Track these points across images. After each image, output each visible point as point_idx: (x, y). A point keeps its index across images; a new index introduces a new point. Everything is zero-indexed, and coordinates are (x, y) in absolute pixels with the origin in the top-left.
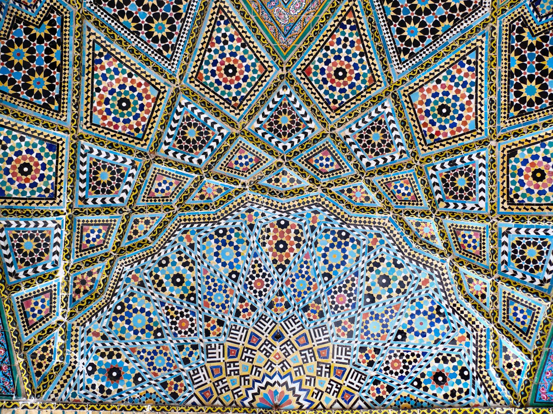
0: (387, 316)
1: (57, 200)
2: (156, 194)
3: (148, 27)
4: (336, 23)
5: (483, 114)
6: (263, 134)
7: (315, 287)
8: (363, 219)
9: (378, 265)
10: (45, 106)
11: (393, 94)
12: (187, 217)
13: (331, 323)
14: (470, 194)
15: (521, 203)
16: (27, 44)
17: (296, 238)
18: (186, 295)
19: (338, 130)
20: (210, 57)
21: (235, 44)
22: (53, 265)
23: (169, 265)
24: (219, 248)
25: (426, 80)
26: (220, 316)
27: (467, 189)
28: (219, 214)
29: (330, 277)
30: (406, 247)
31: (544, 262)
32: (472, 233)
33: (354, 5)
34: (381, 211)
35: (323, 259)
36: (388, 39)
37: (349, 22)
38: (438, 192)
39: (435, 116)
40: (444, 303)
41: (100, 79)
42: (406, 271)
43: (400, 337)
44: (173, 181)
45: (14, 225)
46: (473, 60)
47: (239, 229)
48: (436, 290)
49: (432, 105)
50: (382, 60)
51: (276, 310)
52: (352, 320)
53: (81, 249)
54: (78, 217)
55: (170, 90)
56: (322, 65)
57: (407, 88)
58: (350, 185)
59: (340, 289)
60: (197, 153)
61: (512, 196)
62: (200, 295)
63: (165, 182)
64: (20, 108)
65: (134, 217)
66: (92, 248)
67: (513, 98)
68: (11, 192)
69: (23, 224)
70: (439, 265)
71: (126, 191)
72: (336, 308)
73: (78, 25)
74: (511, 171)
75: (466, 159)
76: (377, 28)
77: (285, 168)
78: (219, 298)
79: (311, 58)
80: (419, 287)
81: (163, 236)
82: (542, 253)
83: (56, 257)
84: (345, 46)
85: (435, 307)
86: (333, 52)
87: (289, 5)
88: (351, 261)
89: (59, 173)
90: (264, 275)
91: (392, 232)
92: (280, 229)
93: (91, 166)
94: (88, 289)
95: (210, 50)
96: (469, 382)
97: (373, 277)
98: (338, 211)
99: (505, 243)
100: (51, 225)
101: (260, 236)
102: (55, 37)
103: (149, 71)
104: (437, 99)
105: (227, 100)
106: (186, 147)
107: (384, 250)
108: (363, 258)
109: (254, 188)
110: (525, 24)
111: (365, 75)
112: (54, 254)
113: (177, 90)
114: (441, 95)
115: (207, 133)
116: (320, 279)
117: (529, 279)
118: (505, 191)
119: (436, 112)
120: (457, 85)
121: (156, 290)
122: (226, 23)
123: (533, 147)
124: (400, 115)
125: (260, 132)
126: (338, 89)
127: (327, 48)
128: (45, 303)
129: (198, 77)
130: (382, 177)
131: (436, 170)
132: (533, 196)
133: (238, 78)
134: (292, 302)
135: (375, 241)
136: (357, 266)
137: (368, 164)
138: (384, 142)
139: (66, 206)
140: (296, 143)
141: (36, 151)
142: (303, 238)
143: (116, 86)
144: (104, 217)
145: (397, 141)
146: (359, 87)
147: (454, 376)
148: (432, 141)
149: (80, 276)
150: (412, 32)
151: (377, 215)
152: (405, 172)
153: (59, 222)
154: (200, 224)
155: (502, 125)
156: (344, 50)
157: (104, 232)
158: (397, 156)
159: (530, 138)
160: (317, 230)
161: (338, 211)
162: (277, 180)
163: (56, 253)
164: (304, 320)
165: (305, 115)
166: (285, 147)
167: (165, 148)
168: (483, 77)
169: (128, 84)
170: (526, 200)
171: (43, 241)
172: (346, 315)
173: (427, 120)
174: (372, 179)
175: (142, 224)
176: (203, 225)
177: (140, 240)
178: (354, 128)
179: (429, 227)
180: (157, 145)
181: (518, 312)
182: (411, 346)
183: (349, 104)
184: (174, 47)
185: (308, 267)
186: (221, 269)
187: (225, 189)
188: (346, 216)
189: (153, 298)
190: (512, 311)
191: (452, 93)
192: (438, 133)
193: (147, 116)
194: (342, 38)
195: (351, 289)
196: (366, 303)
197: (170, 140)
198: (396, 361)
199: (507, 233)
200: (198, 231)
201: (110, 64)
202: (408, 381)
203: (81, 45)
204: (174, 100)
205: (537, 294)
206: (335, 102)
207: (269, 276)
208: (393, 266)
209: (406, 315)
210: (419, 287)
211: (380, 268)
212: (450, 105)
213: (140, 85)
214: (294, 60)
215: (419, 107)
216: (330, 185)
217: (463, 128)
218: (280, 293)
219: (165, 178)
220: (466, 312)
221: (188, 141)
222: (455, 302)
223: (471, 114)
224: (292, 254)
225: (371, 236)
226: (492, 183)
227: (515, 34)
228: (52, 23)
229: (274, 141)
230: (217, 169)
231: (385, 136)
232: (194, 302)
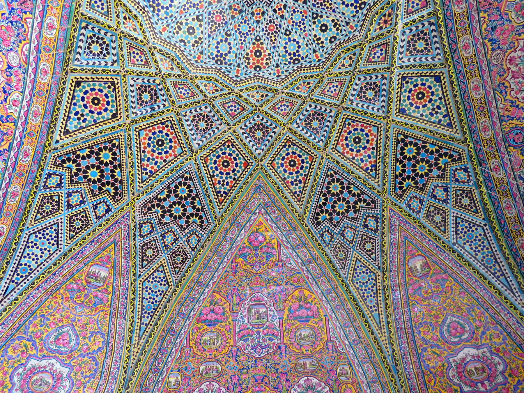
1: (401, 76)
2: (337, 84)
3: (343, 188)
5: (135, 141)
6: (271, 124)
7: (235, 26)
8: (207, 72)
9: (196, 42)
10: (406, 137)
12: (318, 70)
14: (140, 89)
15: (106, 83)
16: (417, 175)
17: (249, 59)
18: (319, 18)
19: (226, 128)
20: (305, 171)
21: (290, 180)
22: (405, 32)
23: (329, 38)
24: (298, 51)
25: (173, 161)
26: (297, 5)
27: (142, 92)
28: (298, 73)
29: (226, 34)
30: (178, 54)
31: (87, 42)
32: (136, 62)
35: (231, 46)
37: (222, 196)
38: (161, 90)
39: (166, 139)
40: (150, 14)
41: (372, 156)
42: (178, 37)
44: (327, 93)
45: (429, 58)
46: (144, 175)
47: (285, 64)
48: (157, 24)
49: (168, 146)
51: (260, 10)
53: (386, 45)
54: (387, 66)
55: (329, 150)
56: (237, 169)
58: (216, 94)
59: (219, 26)
60: (312, 111)
61: (113, 87)
62: (310, 18)
63: (332, 92)
64: (422, 134)
65: (352, 69)
66: (379, 46)
67: (118, 152)
68: (430, 80)
69: (423, 59)
70: (156, 41)
71: (357, 85)
72: (221, 12)
73: (385, 187)
74: (115, 104)
77: (258, 104)
78: (297, 17)
80: (168, 26)
81: (333, 57)
83: (403, 38)
86: (231, 177)
88: (213, 45)
89: (399, 94)
90: (268, 35)
91: (189, 64)
92: (259, 65)
93: (379, 100)
94: (383, 18)
95: (305, 175)
97: (198, 34)
98: (223, 78)
99: (115, 55)
100: (405, 60)
101: (271, 60)
102: (399, 179)
103: (342, 161)
104: (165, 150)
105: (294, 145)
106: (319, 115)
107: (192, 52)
108: (206, 46)
109: (276, 90)
110: (114, 197)
111: (211, 163)
112: (404, 40)
113: (325, 150)
115: (306, 124)
116: (233, 32)
117: (96, 30)
118: (117, 91)
120: (153, 159)
121: (338, 20)
122: (296, 192)
123: (101, 120)
124: (188, 139)
125: (274, 126)
126: (227, 155)
127: (234, 179)
128: (412, 5)
129: (312, 158)
130: (197, 100)
131: (163, 104)
132: (99, 88)
133: (288, 159)
134: (250, 16)
135: (199, 58)
136: (209, 41)
137: (206, 108)
138: (197, 122)
139: (395, 73)
140: (251, 120)
141: (413, 108)
143: (362, 151)
144: (371, 67)
145: (189, 123)
146: (214, 156)
148: (167, 123)
149: (388, 26)
150: (183, 191)
151: (199, 75)
152: (183, 103)
153: (400, 62)
154: (310, 66)
155: (123, 134)
156: (224, 178)
157: (371, 57)
158: (188, 113)
159: (104, 126)
160: (236, 65)
161: (223, 78)
162: (262, 96)
163: (402, 41)
164: (242, 4)
165: (246, 138)
166: (258, 117)
167: (332, 114)
168: (137, 164)
169: (354, 153)
170: (103, 85)
171: (411, 49)
172: (214, 7)
173: (171, 137)
174: (203, 98)
175: (347, 64)
176: (308, 66)
177: (348, 53)
178: (216, 130)
179: (165, 66)
180: (337, 115)
181: (101, 6)
184: (327, 176)
185: (241, 40)
186: (296, 37)
187: (294, 89)
188: (218, 74)
189: (340, 15)
190: (105, 7)
191: (156, 154)
192: (163, 128)
193: (343, 133)
194: (225, 186)
195: (212, 25)
196: (202, 15)
197: (329, 119)
199: (114, 62)
200: (311, 62)
201: (366, 165)
203: (384, 175)
204: (327, 144)
205: (90, 18)
206: (228, 146)
207: (265, 34)
208: (186, 41)
209: (175, 6)
211: (194, 40)
212: (157, 146)
213: (348, 153)
214: (254, 171)
215: (176, 145)
216: (230, 94)
217: (147, 132)
218: (258, 22)
219: (332, 94)
220: (136, 7)
221: (317, 119)
222: (144, 15)
223: (143, 141)
224: (251, 49)
225: (202, 61)
227: (119, 191)
228: (401, 188)
229: (265, 121)
230: (300, 101)
231: (197, 126)
232: (313, 13)
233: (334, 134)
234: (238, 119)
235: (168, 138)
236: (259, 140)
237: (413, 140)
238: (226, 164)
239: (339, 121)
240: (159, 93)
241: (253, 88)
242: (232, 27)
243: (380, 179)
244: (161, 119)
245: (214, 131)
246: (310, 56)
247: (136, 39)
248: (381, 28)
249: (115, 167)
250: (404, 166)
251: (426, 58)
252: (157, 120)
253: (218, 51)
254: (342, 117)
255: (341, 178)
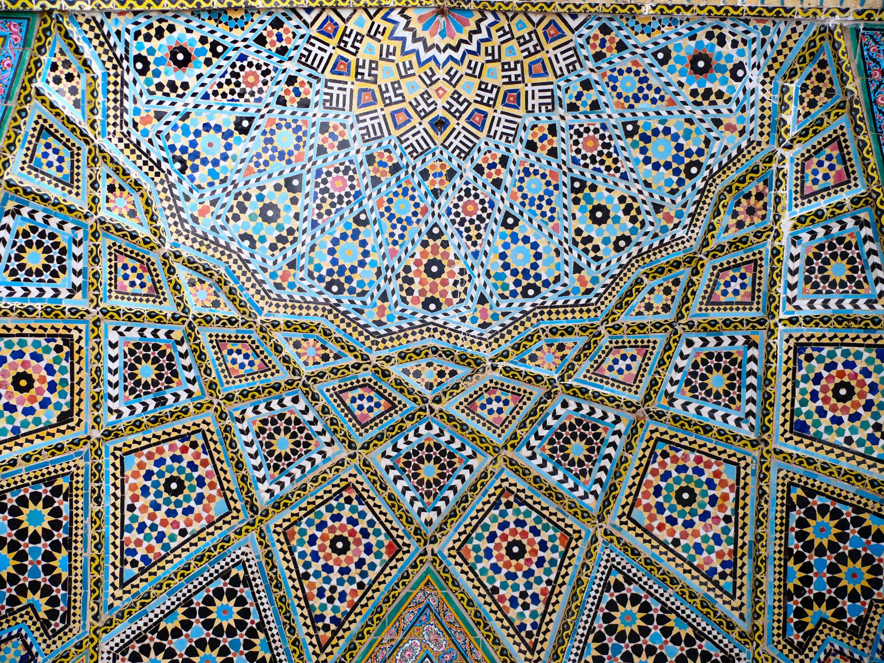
0: (266, 156)
1: (792, 342)
2: (634, 351)
3: (648, 619)
4: (346, 625)
5: (112, 480)
6: (463, 448)
7: (380, 203)
8: (304, 312)
9: (281, 239)
10: (812, 493)
11: (256, 513)
13: (355, 146)
14: (132, 352)
15: (51, 338)
17: (410, 281)
18: (587, 190)
20: (548, 572)
21: (508, 593)
22: (798, 238)
23: (613, 239)
24: (535, 266)
26: (533, 158)
27: (138, 360)
28: (534, 320)
29: (357, 220)
30: (234, 267)
31: (15, 243)
32: (130, 290)
33: (318, 656)
34: (275, 325)
35: (368, 248)
36: (265, 600)
37: (326, 628)
38: (184, 356)
39: (189, 477)
40: (173, 178)
42: (235, 229)
43: (245, 124)
44: (607, 373)
45: (861, 303)
46: (128, 567)
47: (502, 296)
48: (187, 199)
49: (194, 495)
50: (274, 567)
51: (443, 166)
52: (321, 150)
53: (755, 264)
54: (759, 315)
55: (612, 520)
56: (369, 559)
57: (234, 522)
58: (324, 367)
59: (340, 201)
60: (569, 417)
61: (66, 349)
62: (565, 190)
63: (620, 371)
64: (852, 490)
65: (670, 316)
66: (737, 266)
67: (65, 507)
68: (866, 355)
69: (847, 303)
70: (182, 239)
71: (683, 357)
72: (347, 170)
73: (759, 623)
74: (68, 389)
75: (139, 408)
76: (282, 619)
77: (429, 395)
78: (534, 186)
79: (387, 571)
80: (214, 203)
81: (624, 285)
82: (18, 258)
83: (795, 251)
84: (333, 589)
85: (188, 172)
86: (352, 580)
87: (423, 654)
88: (323, 245)
89: (789, 386)
90: (462, 223)
91: (258, 292)
92: (437, 296)
93: (739, 397)
94: (744, 202)
95: (549, 582)
96: (134, 52)
97: (287, 220)
98: (343, 326)
99: (77, 273)
100: (802, 303)
101: (468, 285)
102: (795, 603)
103: (646, 550)
104: (185, 505)
105: (522, 503)
106: (586, 427)
107: (270, 262)
108: (305, 249)
109: (478, 362)
110: (45, 624)
111: (301, 543)
112: (798, 256)
113: (601, 518)
114: (180, 510)
115: (554, 450)
116: (373, 216)
117: (39, 217)
118: (76, 357)
119: (187, 484)
120: (154, 527)
121: (634, 199)
122: (523, 626)
123: (32, 427)
124: (244, 479)
125: (468, 451)
126: (344, 521)
127: (361, 585)
128: (812, 177)
129: (568, 539)
130: (272, 380)
131: (187, 391)
132: (32, 350)
133: (504, 537)
134: (417, 178)
135: (284, 277)
136: (313, 237)
137: (295, 400)
138: (271, 436)
141: (826, 422)
142: (400, 281)
143: (699, 525)
144: (718, 315)
146: (310, 523)
147: (158, 62)
149: (757, 220)
150: (225, 611)
151: (281, 318)
152: (236, 388)
153: (789, 307)
155: (81, 463)
156: (334, 583)
158: (249, 414)
159: (38, 442)
160: (377, 294)
161: (343, 326)
162: (441, 374)
163: (794, 258)
164: (398, 151)
165: (396, 479)
166: (429, 427)
168: (112, 539)
169: (679, 528)
170: (44, 343)
171: (816, 277)
172: (330, 159)
173: (202, 471)
174: (289, 376)
175: (658, 305)
176: (560, 303)
177: (659, 280)
178: (318, 458)
179: (198, 299)
180: (634, 431)
181: (56, 164)
182: (228, 108)
183: (326, 496)
184: (607, 587)
185: (392, 235)
188: (331, 317)
189: (640, 186)
191: (161, 514)
192: (184, 450)
193: (649, 477)
194: (337, 603)
195: (323, 200)
196: (299, 177)
198: (251, 85)
200: (567, 293)
201: (708, 561)
202: (231, 53)
204: (606, 503)
206: (349, 500)
208: (256, 237)
209: (234, 158)
210: (214, 203)
211: (277, 233)
212: (165, 495)
213: (661, 527)
214: (414, 566)
215: (214, 492)
216: (357, 367)
217: (144, 459)
218: (436, 193)
219: (620, 378)
220: (140, 163)
221: (583, 437)
222: (157, 179)
223: (132, 480)
224: (418, 256)
225: (292, 286)
226: (98, 370)
227: (61, 608)
228: (800, 626)
229: (447, 437)
230: (538, 392)
231: (269, 445)
232: (573, 180)
233: (627, 479)
234: (375, 432)
235: (196, 475)
236: (429, 485)
237: (828, 502)
238: (340, 545)
239: (639, 446)
240: (179, 362)
241: (417, 352)
242: (371, 203)
243: (745, 599)
244: (179, 426)
245: (312, 461)
246: (566, 280)
247: (134, 237)
248: (740, 225)
249: (56, 546)
250: (807, 568)
251: (854, 303)
252: (169, 430)
253: (334, 262)
254: (647, 435)
255: (642, 594)
